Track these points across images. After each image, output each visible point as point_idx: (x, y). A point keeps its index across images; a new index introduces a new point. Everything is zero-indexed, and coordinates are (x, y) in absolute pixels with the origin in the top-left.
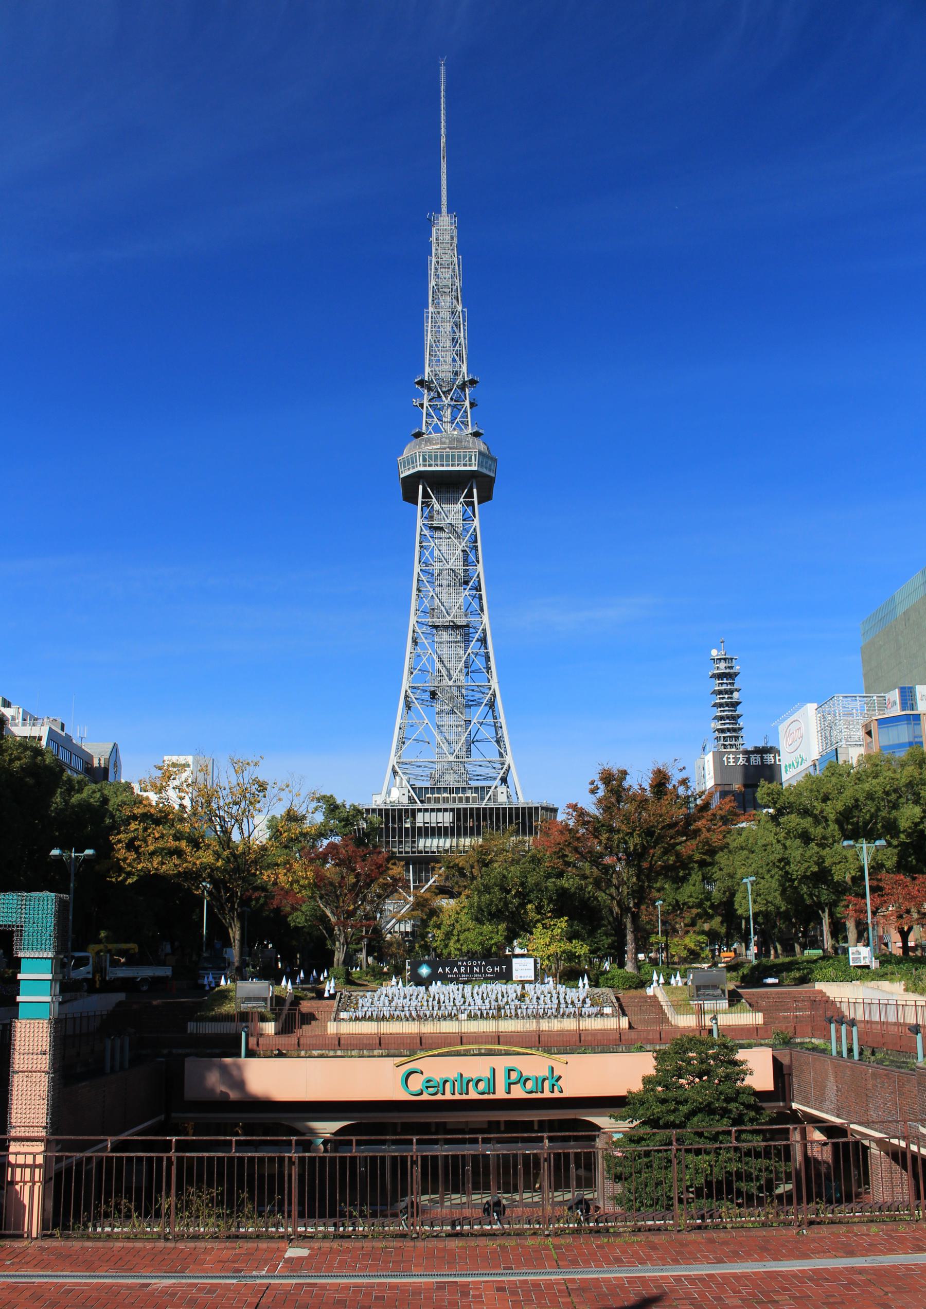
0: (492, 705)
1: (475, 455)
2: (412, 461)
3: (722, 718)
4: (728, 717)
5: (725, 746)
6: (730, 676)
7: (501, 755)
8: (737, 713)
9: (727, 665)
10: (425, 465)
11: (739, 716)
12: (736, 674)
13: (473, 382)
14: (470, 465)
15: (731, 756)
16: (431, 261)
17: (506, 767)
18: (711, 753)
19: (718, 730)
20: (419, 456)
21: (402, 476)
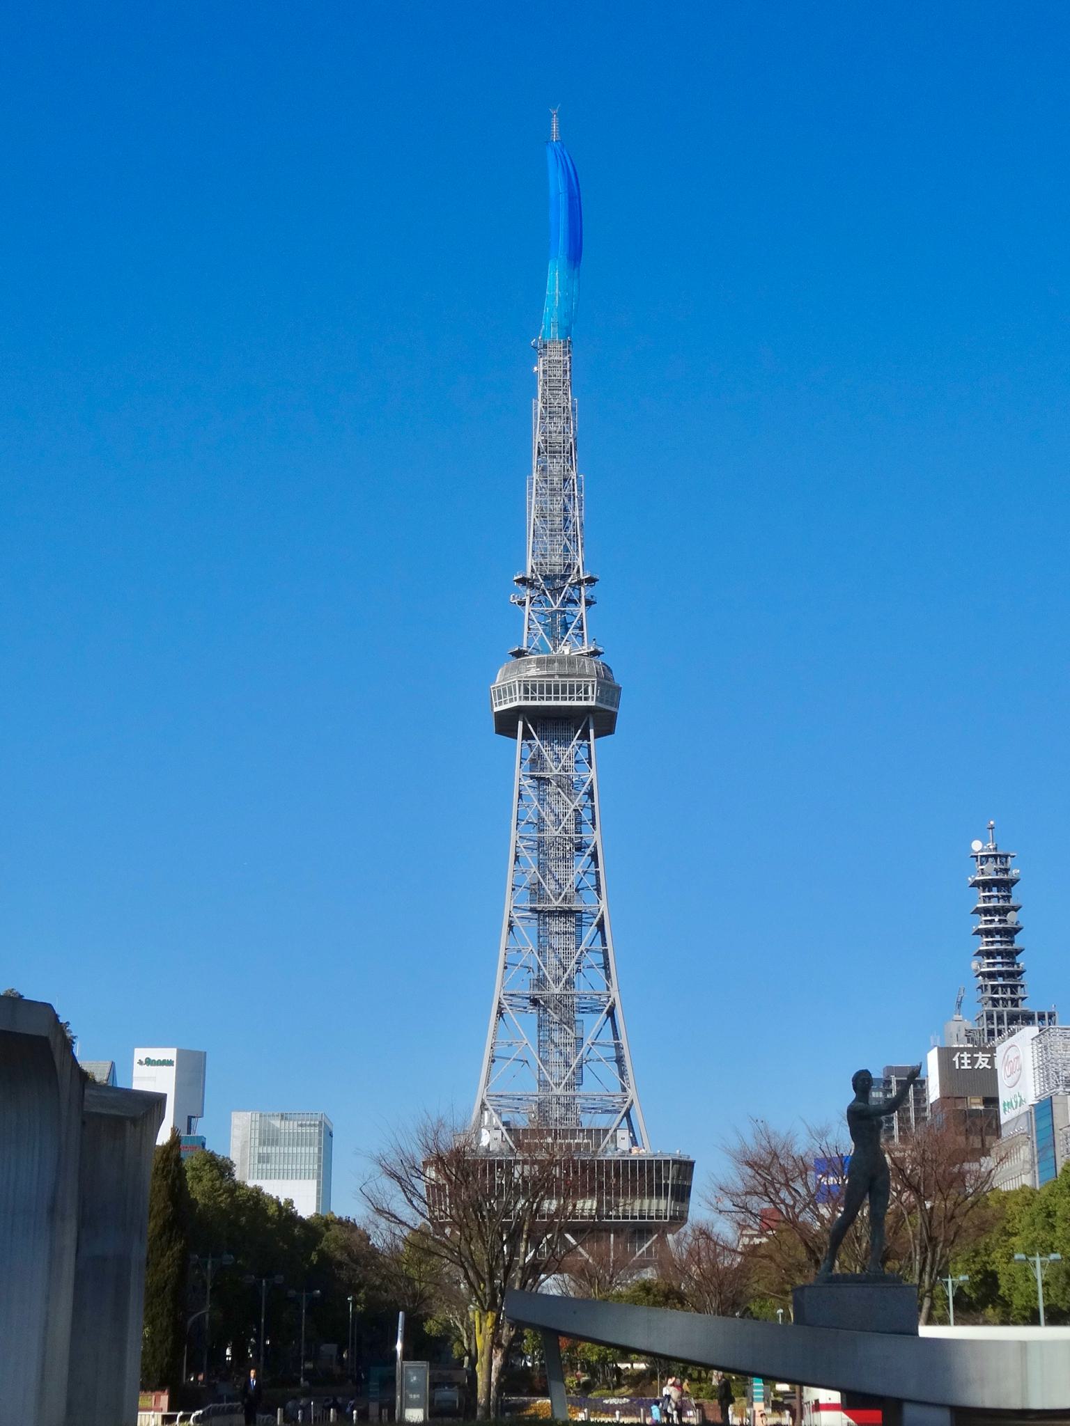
0: (611, 1013)
1: (593, 686)
2: (507, 691)
3: (989, 954)
4: (999, 953)
5: (995, 1002)
6: (1006, 885)
7: (624, 1090)
8: (1015, 946)
9: (999, 866)
10: (526, 698)
11: (1018, 952)
12: (1013, 882)
13: (591, 581)
14: (586, 699)
15: (965, 1055)
16: (536, 406)
17: (629, 1101)
18: (936, 1049)
19: (982, 974)
20: (520, 685)
21: (496, 709)
